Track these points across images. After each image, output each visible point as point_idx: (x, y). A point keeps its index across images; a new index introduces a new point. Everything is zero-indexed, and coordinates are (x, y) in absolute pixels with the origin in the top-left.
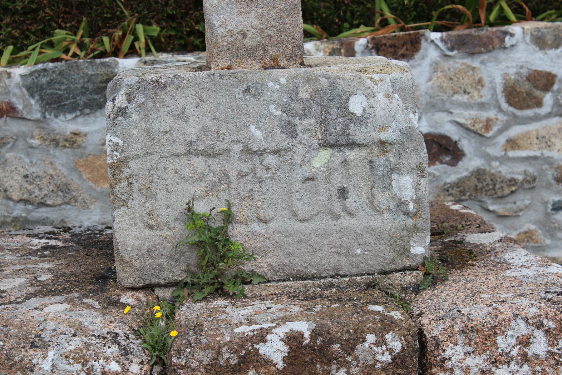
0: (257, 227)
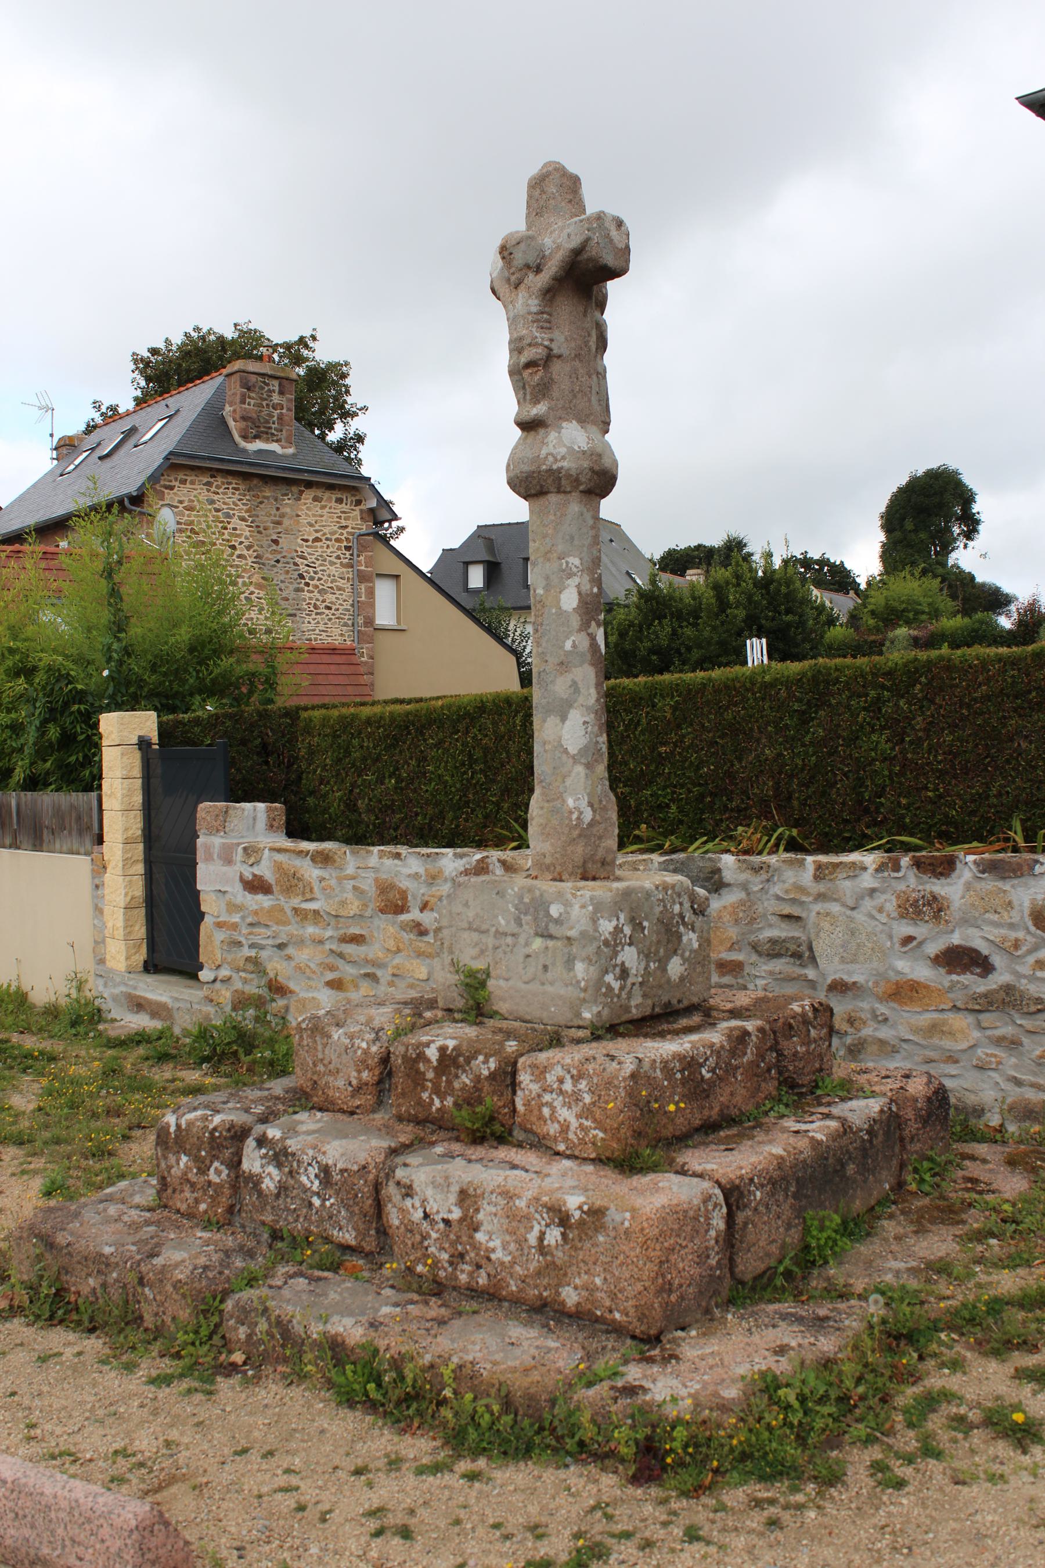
0: (502, 983)
